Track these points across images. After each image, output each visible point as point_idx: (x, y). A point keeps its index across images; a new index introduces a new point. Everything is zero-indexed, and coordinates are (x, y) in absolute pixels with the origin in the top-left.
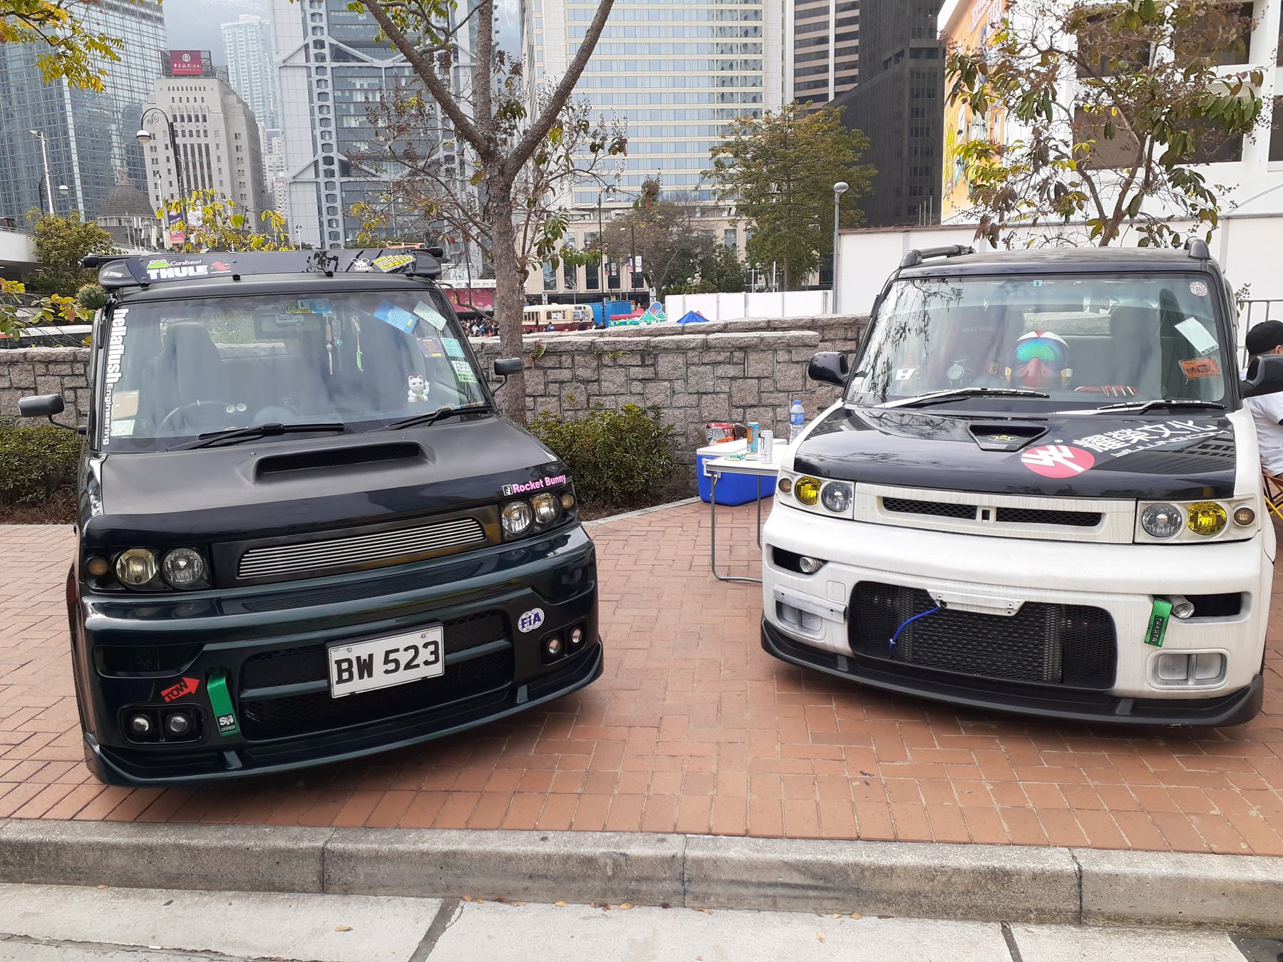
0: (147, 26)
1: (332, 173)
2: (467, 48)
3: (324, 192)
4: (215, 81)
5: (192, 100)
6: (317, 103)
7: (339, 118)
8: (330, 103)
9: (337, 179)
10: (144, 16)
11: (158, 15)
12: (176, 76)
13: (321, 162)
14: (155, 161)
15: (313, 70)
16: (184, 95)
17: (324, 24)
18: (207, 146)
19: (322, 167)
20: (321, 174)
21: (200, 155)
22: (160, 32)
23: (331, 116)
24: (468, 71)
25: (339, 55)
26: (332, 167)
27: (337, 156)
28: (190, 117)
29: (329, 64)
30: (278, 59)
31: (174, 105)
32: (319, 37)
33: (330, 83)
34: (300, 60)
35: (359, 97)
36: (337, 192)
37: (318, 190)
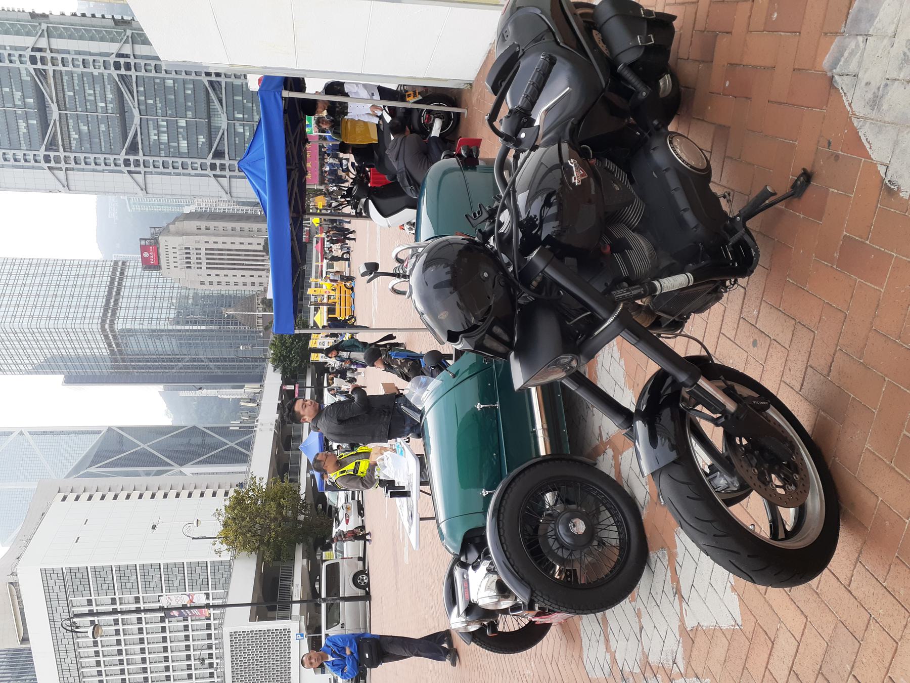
0: (129, 272)
1: (223, 167)
4: (161, 238)
5: (175, 255)
7: (181, 155)
8: (170, 160)
10: (122, 273)
11: (120, 263)
12: (159, 263)
13: (214, 172)
14: (219, 283)
15: (147, 169)
16: (172, 260)
17: (112, 157)
18: (207, 249)
19: (218, 172)
20: (223, 173)
21: (213, 254)
22: (132, 264)
23: (180, 160)
25: (133, 149)
26: (218, 169)
27: (209, 160)
28: (187, 258)
29: (140, 157)
30: (141, 193)
31: (180, 267)
32: (121, 162)
33: (156, 158)
35: (164, 138)
37: (235, 177)
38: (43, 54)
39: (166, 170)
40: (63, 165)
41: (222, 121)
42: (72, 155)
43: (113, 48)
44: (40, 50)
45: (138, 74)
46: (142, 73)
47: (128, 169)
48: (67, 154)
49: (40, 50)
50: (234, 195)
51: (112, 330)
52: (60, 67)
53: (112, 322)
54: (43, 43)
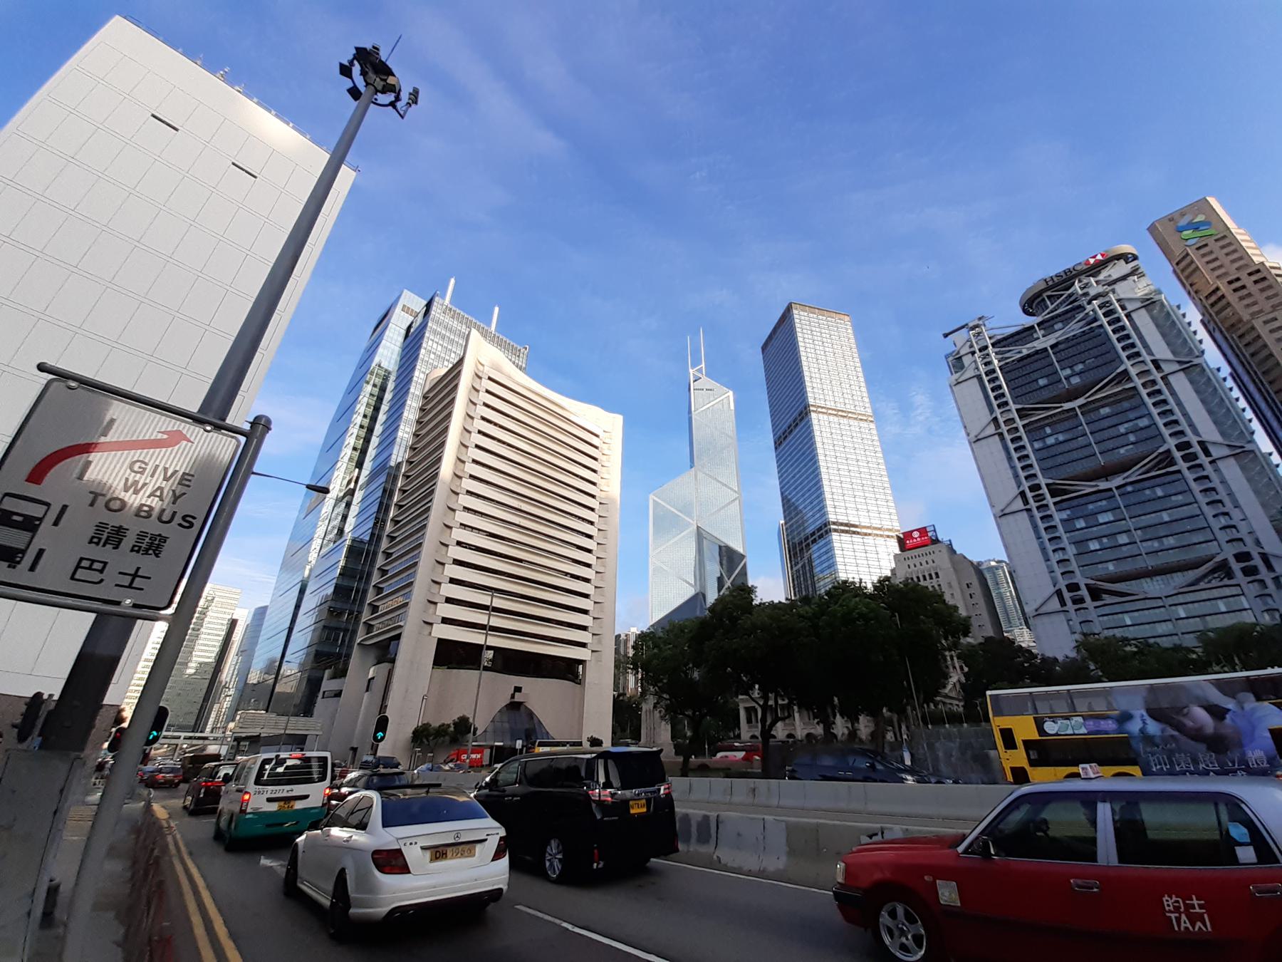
6: (1046, 537)
15: (1035, 510)
16: (917, 561)
19: (1067, 595)
20: (1069, 602)
29: (1050, 500)
34: (1019, 504)
38: (1154, 370)
40: (1004, 429)
44: (1158, 367)
45: (1186, 473)
46: (1190, 476)
47: (1027, 491)
48: (1021, 429)
49: (1158, 367)
51: (827, 532)
52: (1144, 392)
53: (836, 531)
54: (1167, 368)
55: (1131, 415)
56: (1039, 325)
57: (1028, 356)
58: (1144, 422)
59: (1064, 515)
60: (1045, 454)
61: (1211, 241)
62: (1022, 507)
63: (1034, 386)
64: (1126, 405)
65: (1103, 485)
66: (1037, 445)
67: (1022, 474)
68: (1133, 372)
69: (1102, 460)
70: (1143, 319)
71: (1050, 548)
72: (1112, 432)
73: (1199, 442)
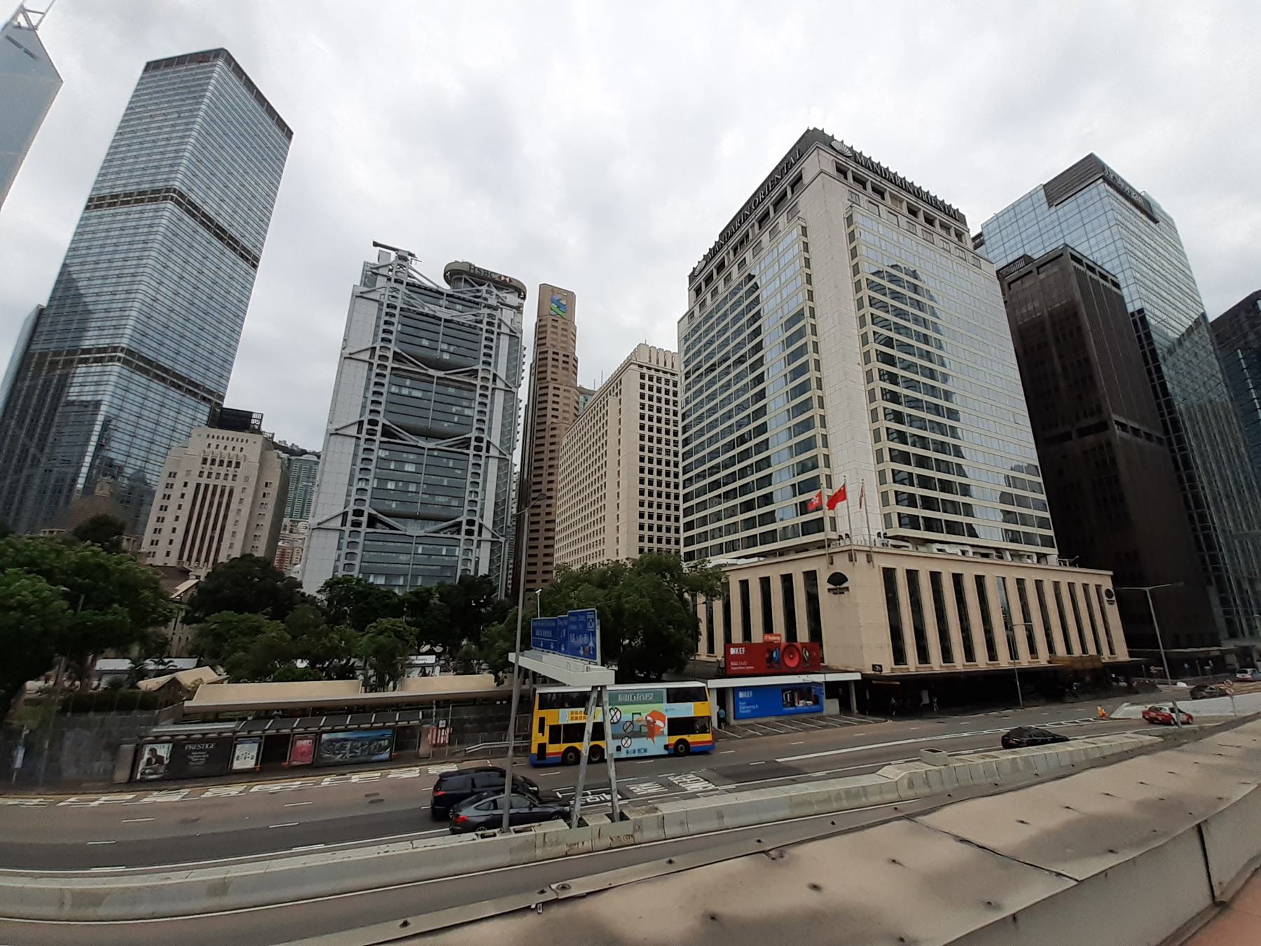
1: (356, 524)
2: (498, 445)
3: (347, 539)
6: (359, 465)
9: (364, 529)
13: (351, 513)
15: (363, 441)
19: (350, 518)
20: (349, 523)
24: (496, 461)
25: (386, 432)
27: (367, 509)
29: (378, 437)
34: (353, 431)
36: (360, 540)
37: (341, 538)
39: (359, 460)
41: (414, 529)
42: (387, 372)
43: (496, 440)
44: (494, 380)
46: (472, 460)
49: (494, 380)
50: (316, 533)
52: (479, 391)
54: (500, 384)
55: (465, 403)
56: (448, 295)
57: (427, 315)
58: (467, 412)
59: (383, 454)
60: (395, 399)
61: (560, 321)
62: (355, 433)
63: (416, 341)
64: (465, 394)
65: (422, 443)
66: (394, 389)
67: (370, 407)
68: (480, 374)
69: (430, 424)
70: (505, 341)
71: (357, 475)
72: (447, 408)
73: (489, 443)
